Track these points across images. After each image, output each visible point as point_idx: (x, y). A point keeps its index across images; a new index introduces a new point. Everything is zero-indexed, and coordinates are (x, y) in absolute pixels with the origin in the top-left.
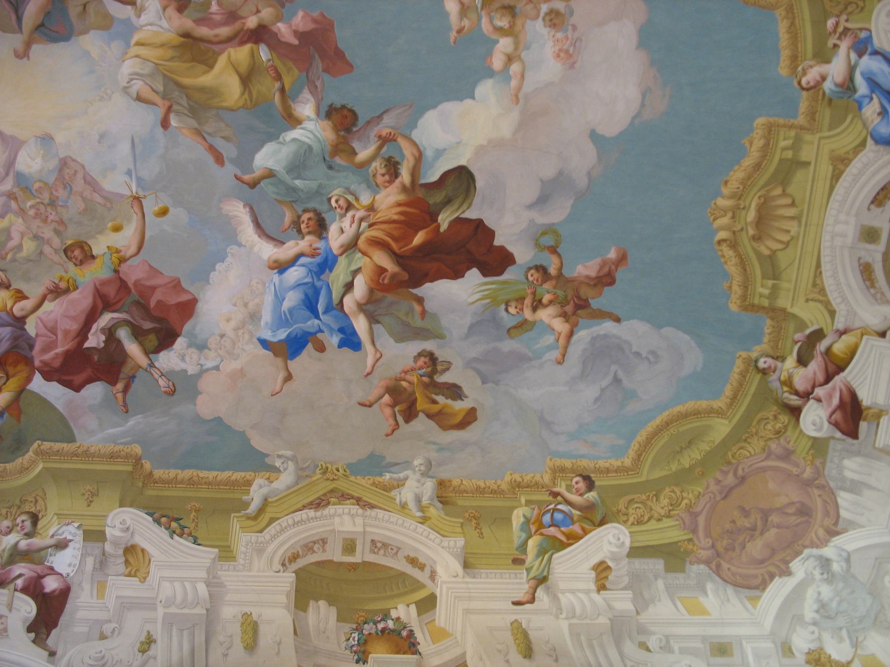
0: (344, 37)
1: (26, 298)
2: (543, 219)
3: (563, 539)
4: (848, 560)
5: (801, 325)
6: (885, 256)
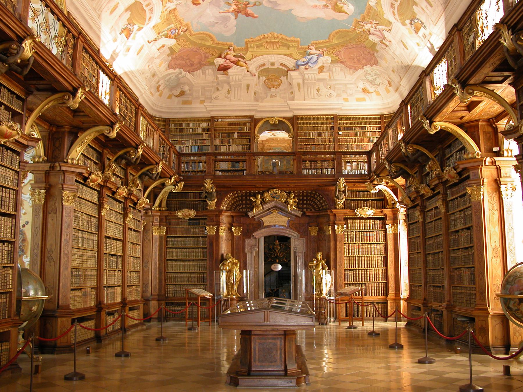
2: (264, 2)
3: (169, 36)
4: (183, 77)
5: (245, 55)
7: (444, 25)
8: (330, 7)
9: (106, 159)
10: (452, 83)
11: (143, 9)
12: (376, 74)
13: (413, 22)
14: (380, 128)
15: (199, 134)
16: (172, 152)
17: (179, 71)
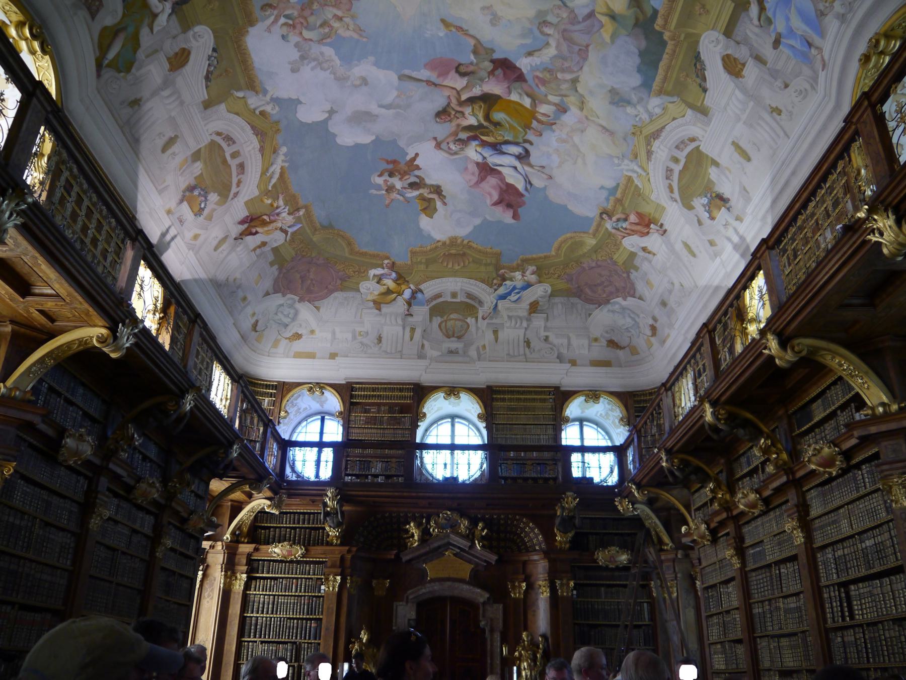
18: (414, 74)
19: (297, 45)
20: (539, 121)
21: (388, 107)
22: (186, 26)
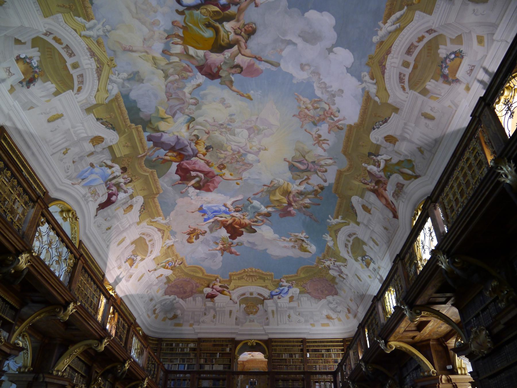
0: (289, 218)
1: (204, 156)
4: (177, 303)
6: (248, 297)
7: (389, 260)
8: (297, 247)
9: (94, 373)
10: (401, 305)
11: (146, 244)
12: (337, 303)
13: (364, 259)
14: (343, 350)
15: (186, 354)
16: (160, 369)
17: (174, 298)
18: (269, 66)
19: (334, 104)
20: (178, 36)
21: (290, 42)
22: (378, 147)
